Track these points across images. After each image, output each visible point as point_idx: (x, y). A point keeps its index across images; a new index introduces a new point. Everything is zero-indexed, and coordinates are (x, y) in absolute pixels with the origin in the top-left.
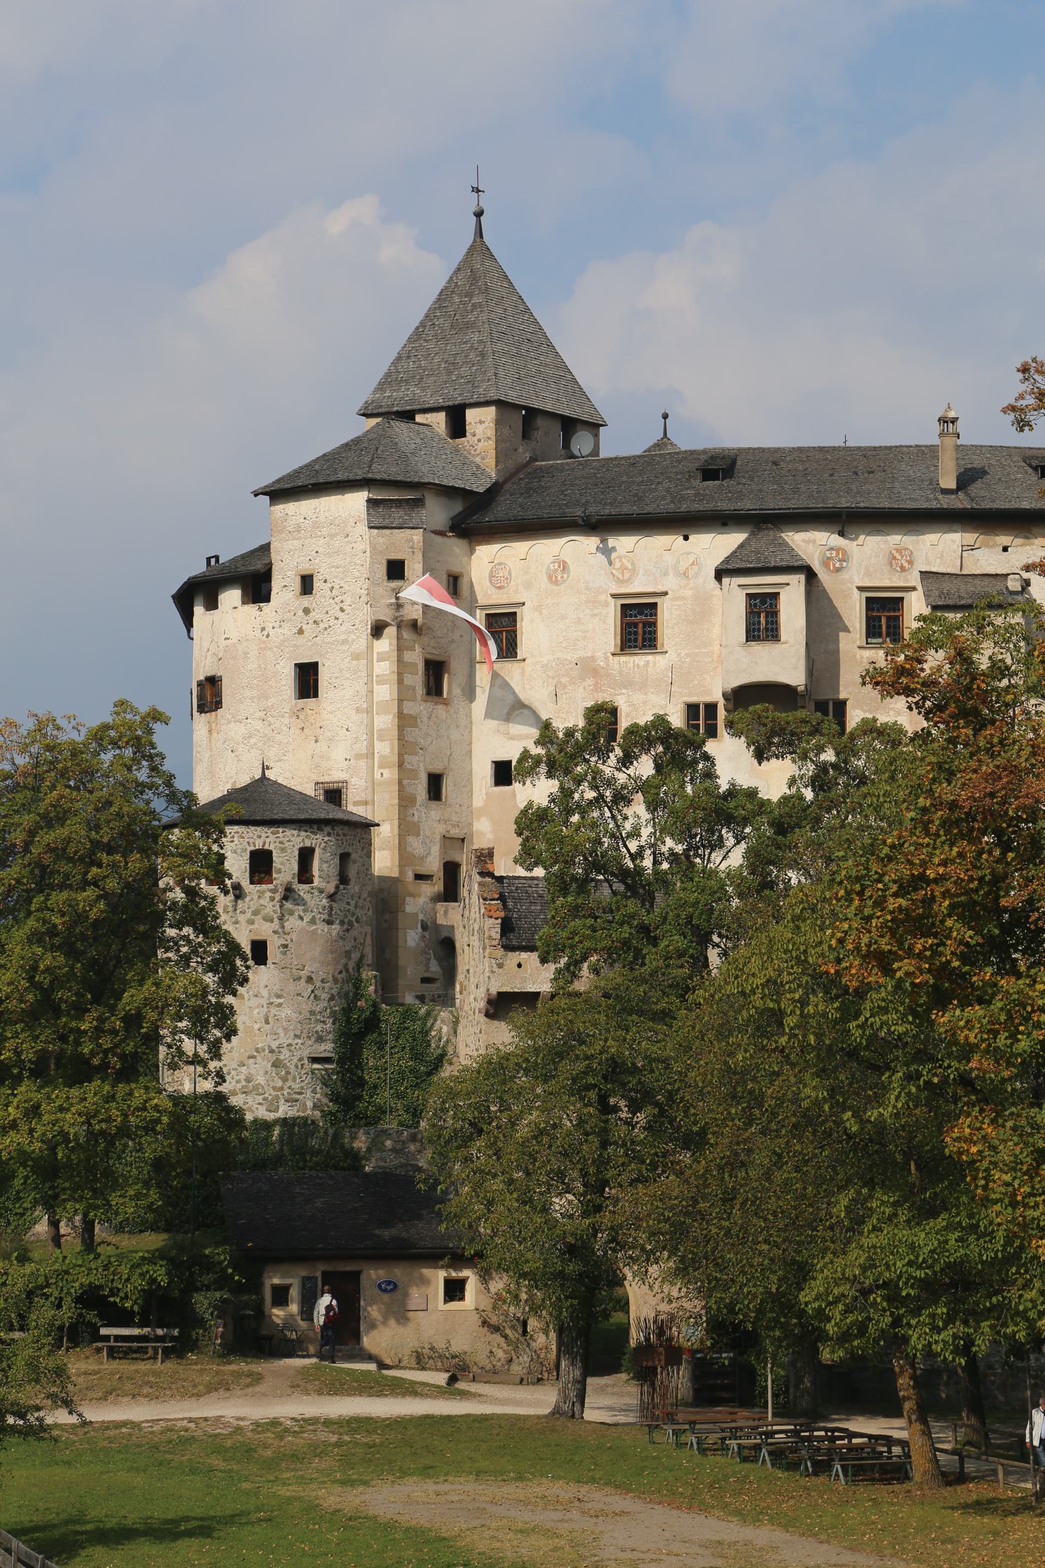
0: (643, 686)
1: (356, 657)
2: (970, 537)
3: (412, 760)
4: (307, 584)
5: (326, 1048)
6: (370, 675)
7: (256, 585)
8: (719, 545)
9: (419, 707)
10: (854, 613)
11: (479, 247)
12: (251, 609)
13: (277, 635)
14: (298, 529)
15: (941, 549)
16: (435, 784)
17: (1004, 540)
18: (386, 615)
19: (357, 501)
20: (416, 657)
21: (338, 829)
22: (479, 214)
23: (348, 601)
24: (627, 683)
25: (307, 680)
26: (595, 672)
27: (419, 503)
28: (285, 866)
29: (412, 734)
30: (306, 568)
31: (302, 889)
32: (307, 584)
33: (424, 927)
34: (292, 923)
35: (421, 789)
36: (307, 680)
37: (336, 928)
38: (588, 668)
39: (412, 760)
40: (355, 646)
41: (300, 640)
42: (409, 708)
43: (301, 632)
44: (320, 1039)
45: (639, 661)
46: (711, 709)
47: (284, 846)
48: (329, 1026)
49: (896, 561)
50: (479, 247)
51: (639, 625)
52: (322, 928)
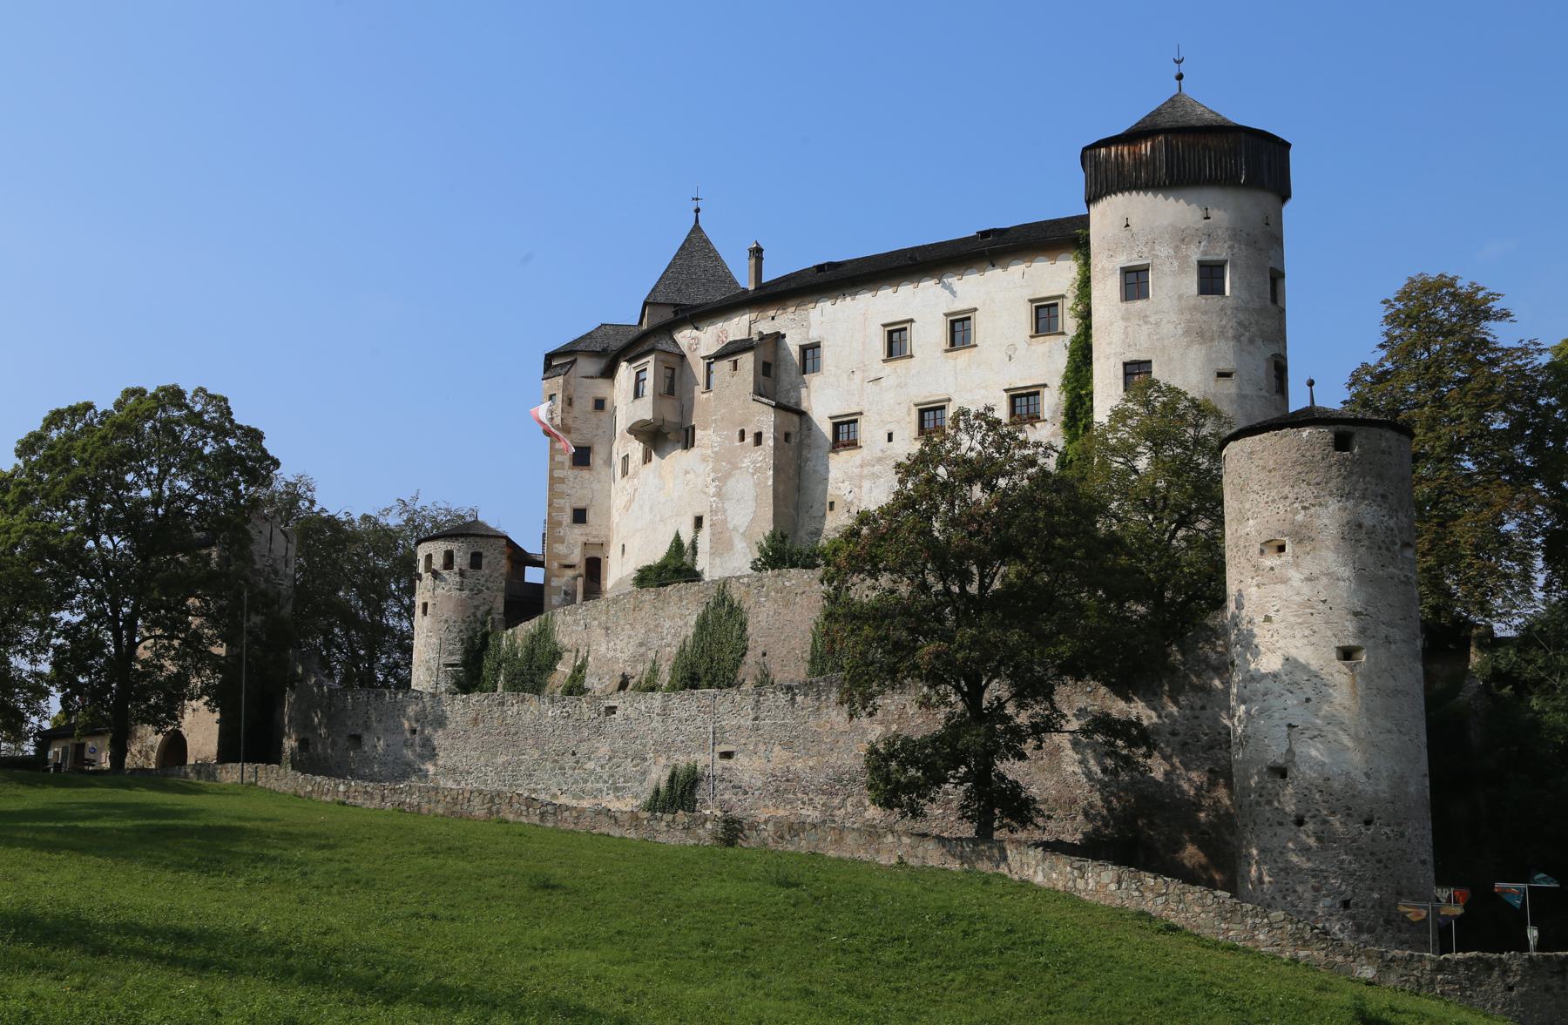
2: (753, 316)
3: (558, 502)
5: (457, 659)
9: (569, 473)
10: (699, 369)
11: (697, 228)
15: (737, 327)
16: (580, 516)
17: (772, 313)
20: (568, 446)
21: (471, 539)
22: (697, 211)
27: (573, 363)
28: (438, 562)
29: (559, 487)
31: (445, 573)
33: (566, 593)
34: (439, 591)
35: (567, 517)
37: (466, 592)
39: (558, 502)
42: (558, 474)
44: (451, 654)
47: (437, 549)
48: (458, 645)
50: (697, 228)
52: (456, 593)
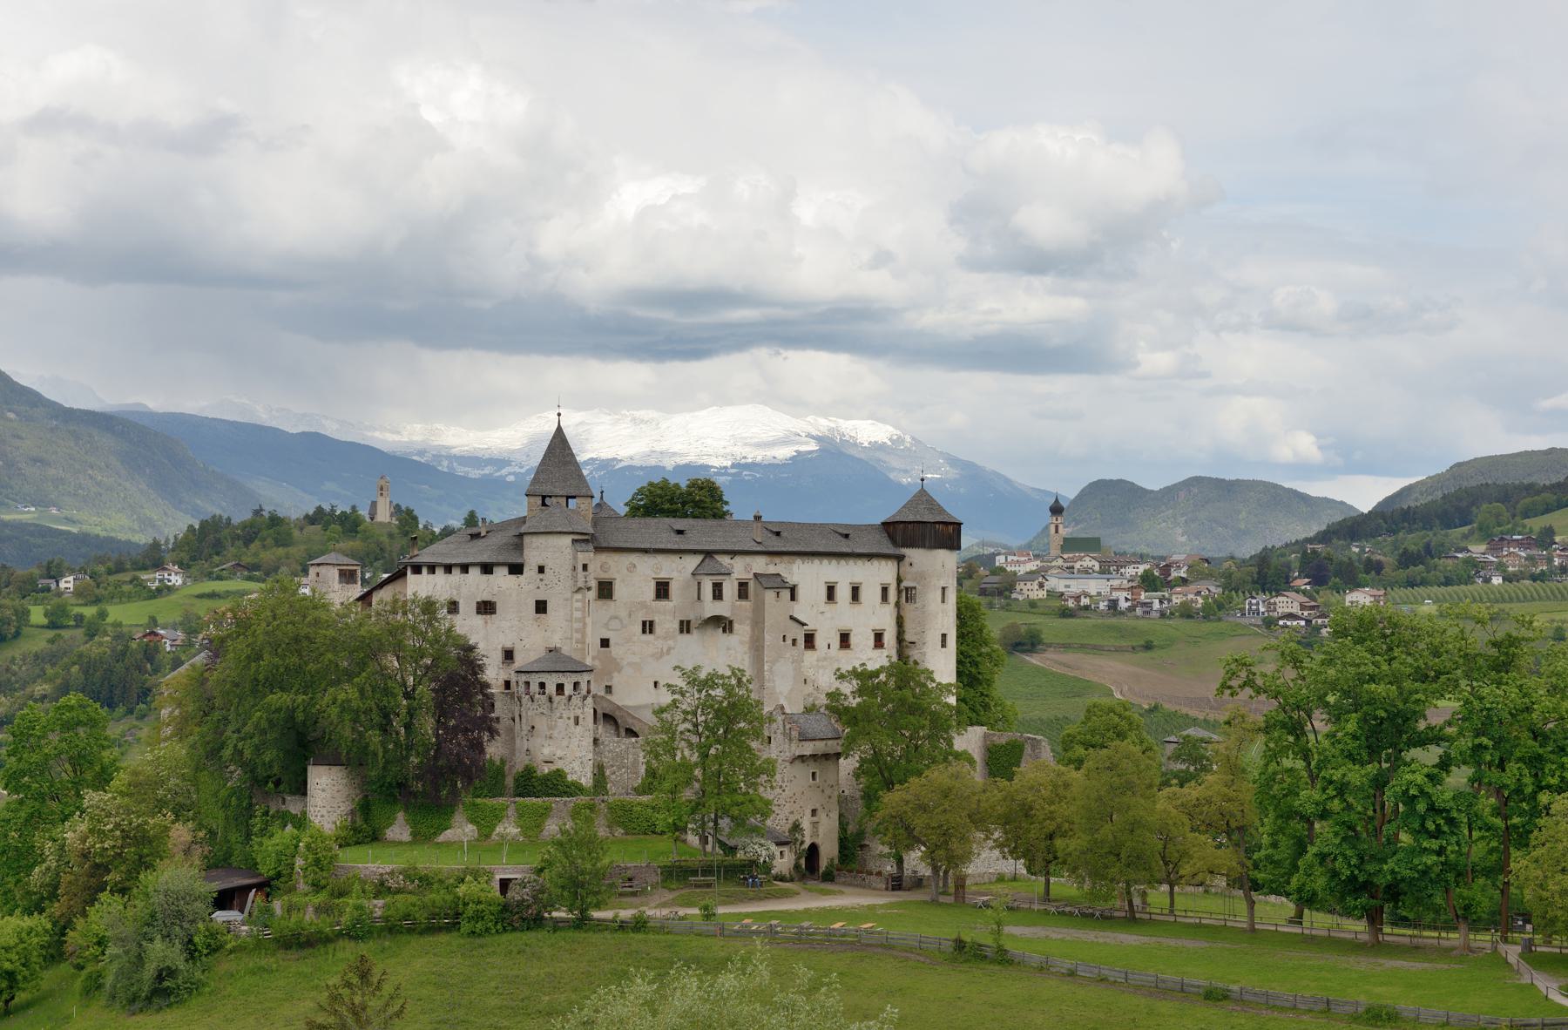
4: (541, 570)
7: (516, 569)
8: (692, 562)
11: (559, 429)
12: (513, 577)
15: (760, 565)
18: (580, 584)
19: (568, 540)
25: (541, 607)
32: (541, 570)
36: (541, 607)
38: (643, 605)
45: (663, 603)
49: (747, 568)
50: (559, 429)
51: (662, 590)
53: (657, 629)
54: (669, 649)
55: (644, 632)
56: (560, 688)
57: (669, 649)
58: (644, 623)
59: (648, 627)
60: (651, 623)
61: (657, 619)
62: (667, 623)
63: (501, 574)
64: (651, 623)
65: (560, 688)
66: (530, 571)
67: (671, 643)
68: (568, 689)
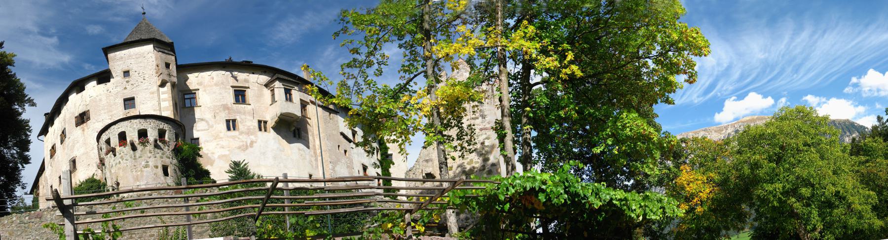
0: (244, 114)
1: (153, 93)
4: (126, 73)
6: (159, 99)
12: (102, 85)
13: (114, 91)
14: (122, 58)
19: (150, 47)
23: (147, 76)
24: (239, 112)
26: (228, 109)
30: (126, 69)
38: (225, 107)
40: (152, 90)
41: (125, 91)
43: (125, 88)
46: (265, 122)
53: (239, 125)
54: (252, 143)
55: (229, 129)
56: (143, 134)
57: (252, 143)
58: (228, 121)
59: (231, 124)
60: (234, 121)
61: (238, 118)
62: (247, 122)
63: (92, 87)
64: (234, 121)
65: (143, 134)
66: (117, 78)
67: (252, 137)
68: (152, 135)
